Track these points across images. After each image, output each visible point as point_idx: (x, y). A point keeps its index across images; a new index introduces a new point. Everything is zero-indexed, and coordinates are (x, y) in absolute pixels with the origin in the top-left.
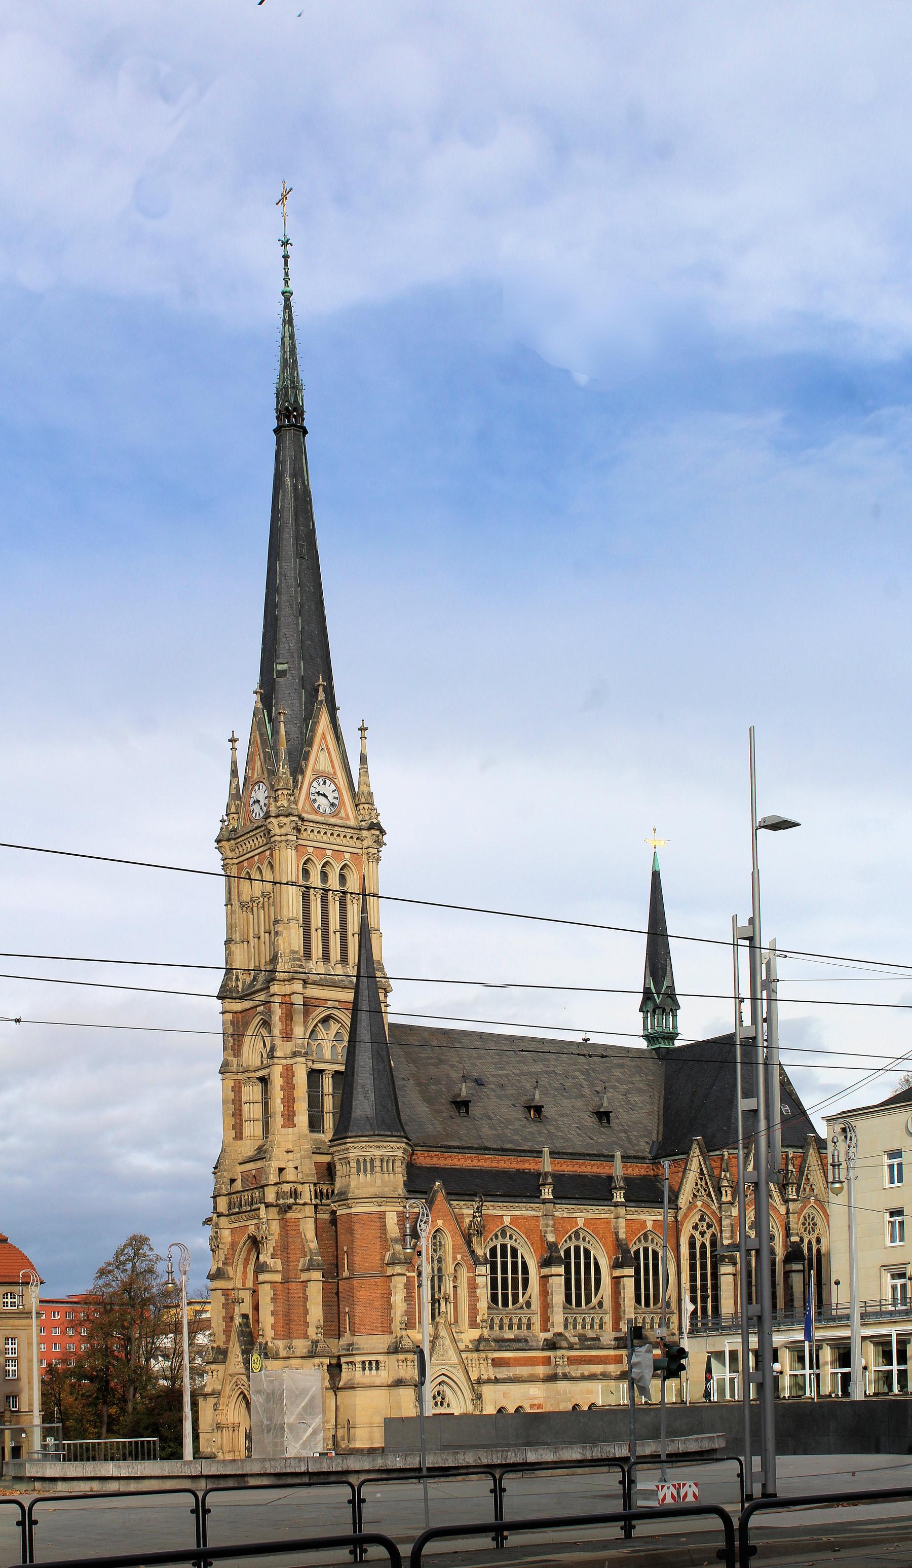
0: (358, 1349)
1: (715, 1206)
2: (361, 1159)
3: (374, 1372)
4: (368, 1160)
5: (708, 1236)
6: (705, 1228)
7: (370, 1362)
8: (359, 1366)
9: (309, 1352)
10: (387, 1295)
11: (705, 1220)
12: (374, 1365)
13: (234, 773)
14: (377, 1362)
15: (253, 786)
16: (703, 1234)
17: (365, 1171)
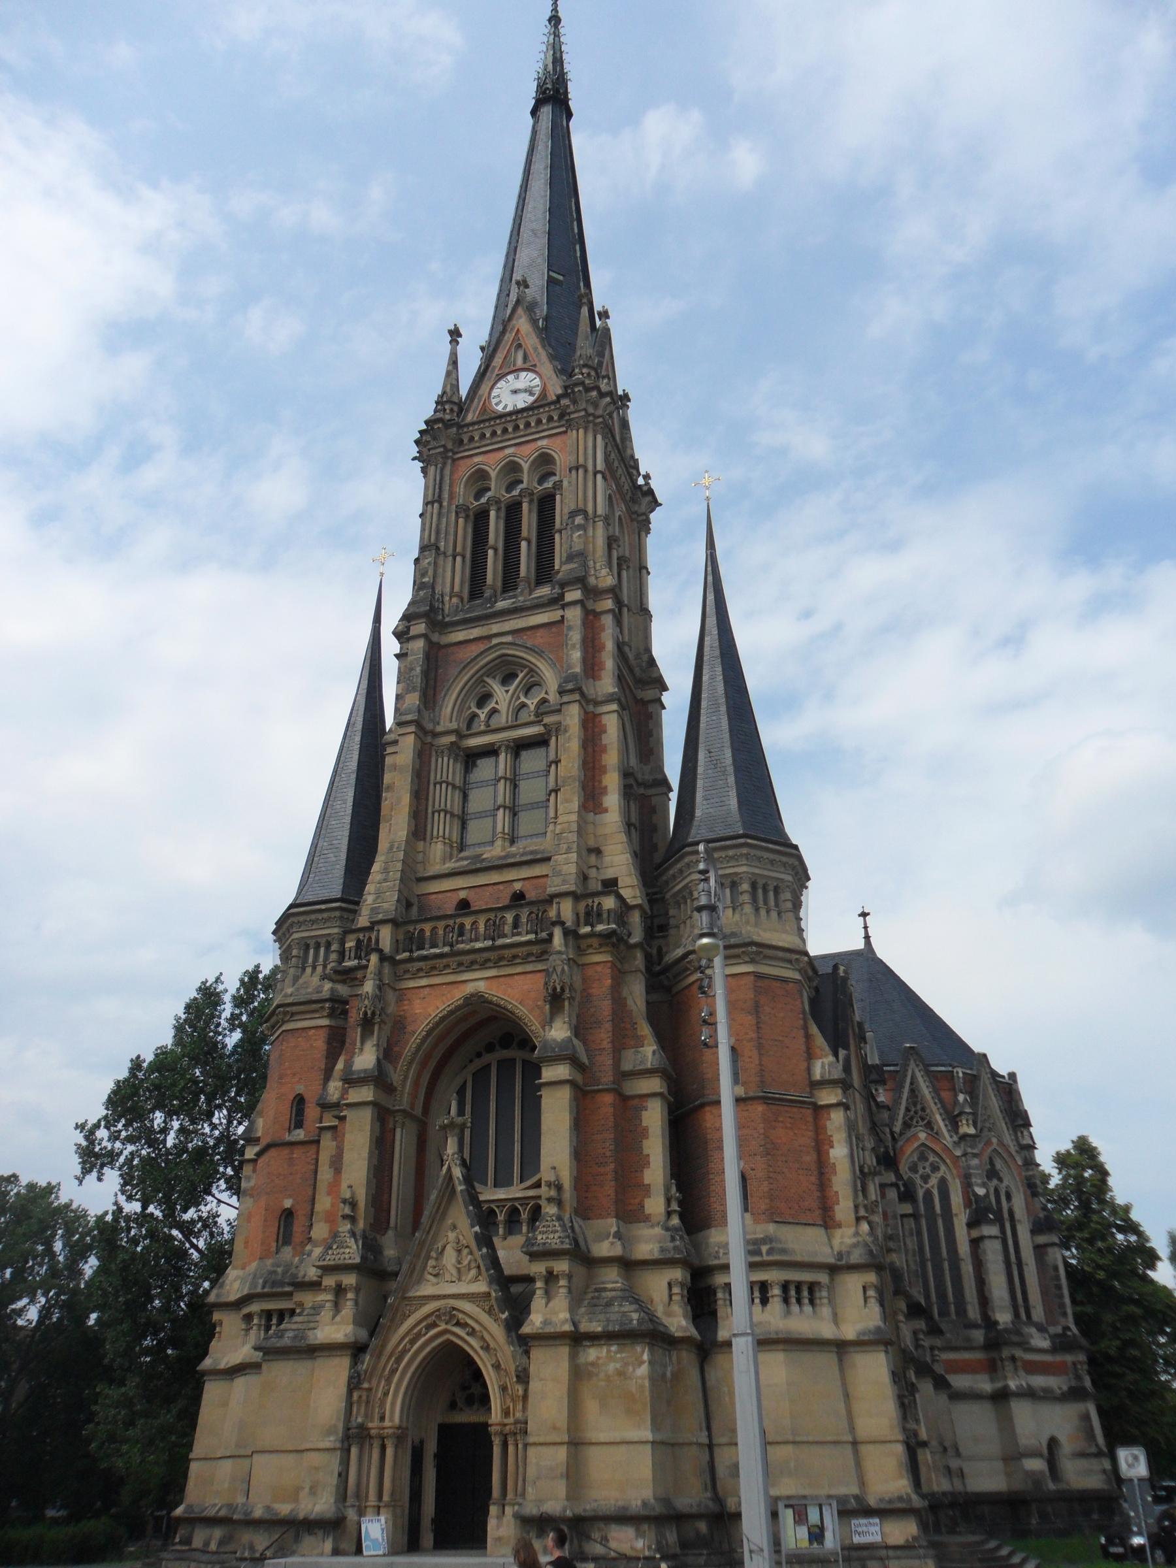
0: (783, 1251)
1: (948, 1139)
2: (761, 882)
3: (808, 1309)
4: (771, 888)
5: (934, 1181)
6: (928, 1170)
7: (799, 1286)
8: (776, 1291)
9: (662, 1250)
10: (821, 1145)
11: (926, 1159)
12: (793, 1293)
13: (454, 362)
14: (812, 1287)
15: (501, 377)
16: (925, 1178)
17: (766, 902)
